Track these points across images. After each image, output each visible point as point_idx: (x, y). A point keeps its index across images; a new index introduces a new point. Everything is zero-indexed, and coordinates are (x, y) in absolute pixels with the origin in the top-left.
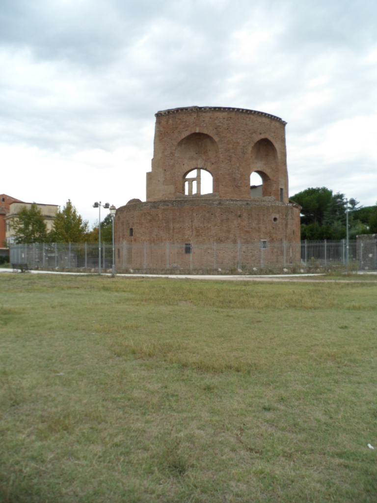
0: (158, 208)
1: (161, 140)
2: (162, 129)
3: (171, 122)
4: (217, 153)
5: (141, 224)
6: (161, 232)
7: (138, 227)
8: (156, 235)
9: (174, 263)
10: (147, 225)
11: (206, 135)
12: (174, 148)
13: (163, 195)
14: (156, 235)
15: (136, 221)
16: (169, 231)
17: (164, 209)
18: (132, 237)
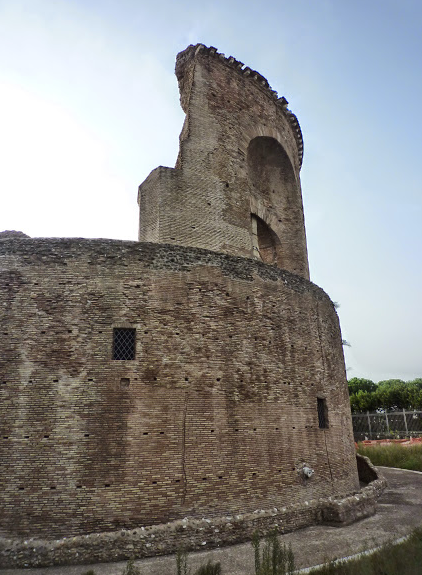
0: (247, 279)
1: (213, 108)
2: (215, 86)
3: (234, 84)
4: (288, 202)
5: (188, 321)
6: (264, 357)
7: (169, 328)
8: (249, 364)
9: (303, 461)
10: (212, 324)
11: (286, 157)
12: (246, 145)
13: (224, 247)
14: (249, 364)
15: (156, 304)
16: (284, 356)
17: (266, 287)
18: (132, 365)
